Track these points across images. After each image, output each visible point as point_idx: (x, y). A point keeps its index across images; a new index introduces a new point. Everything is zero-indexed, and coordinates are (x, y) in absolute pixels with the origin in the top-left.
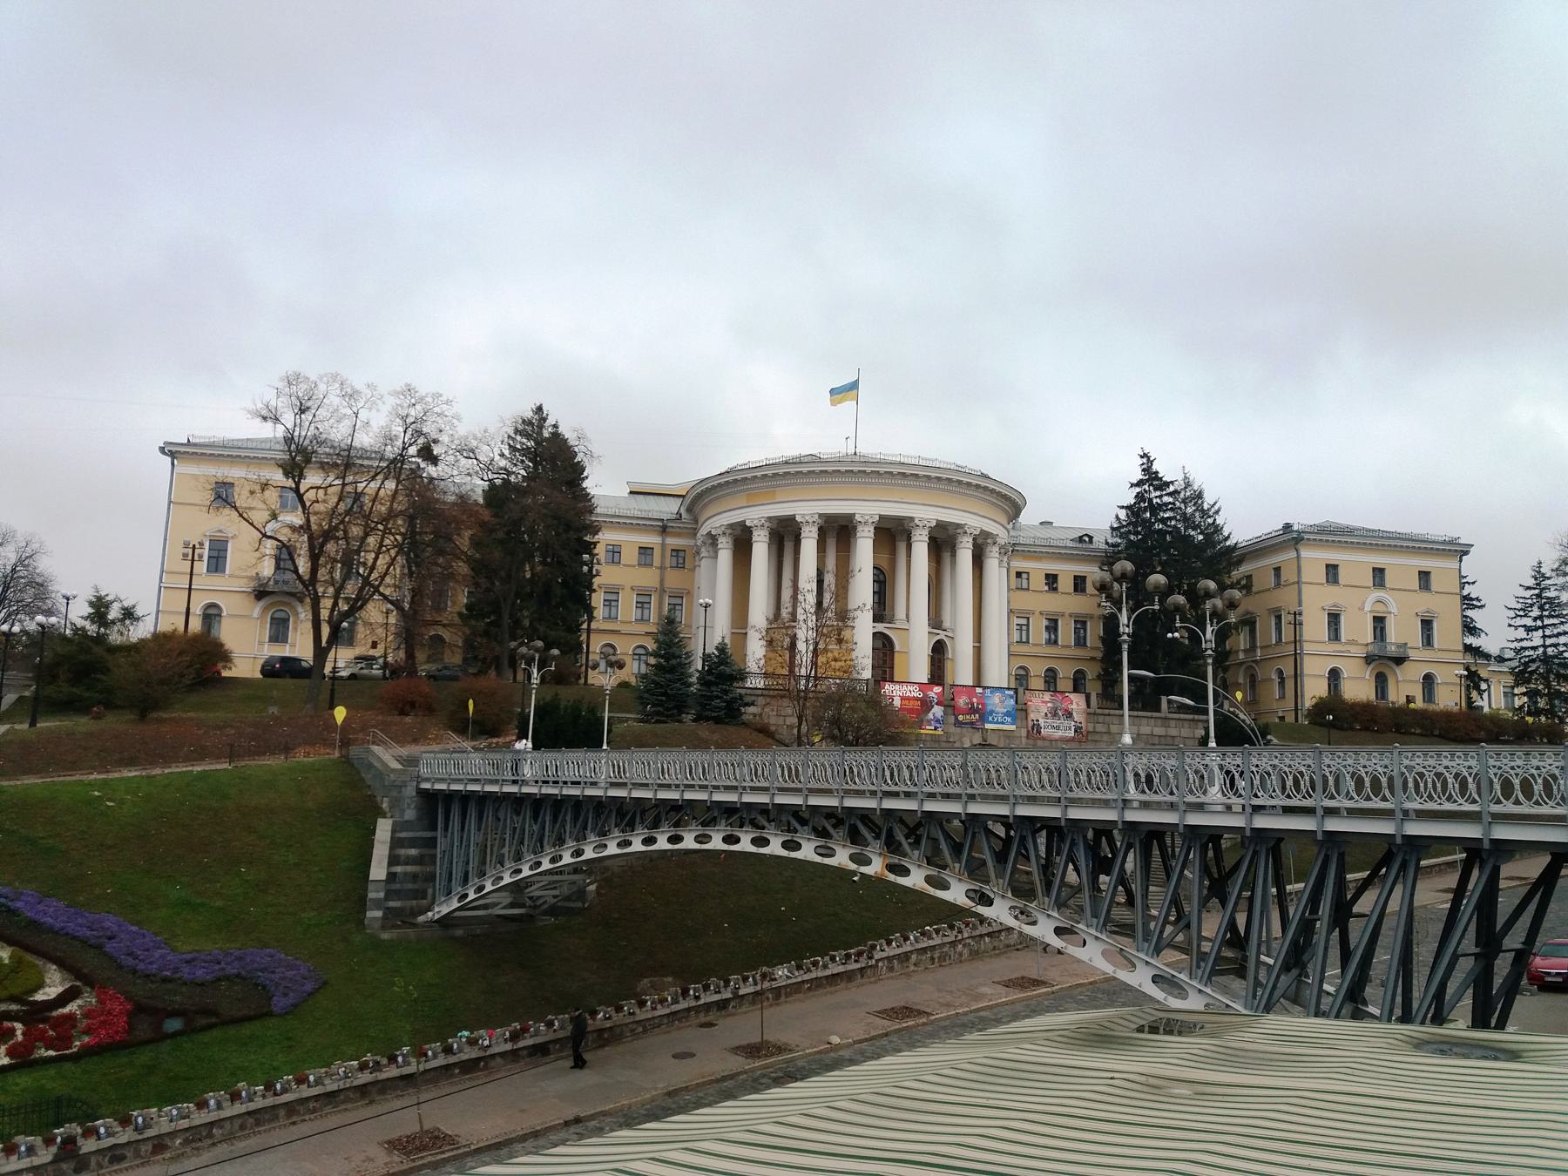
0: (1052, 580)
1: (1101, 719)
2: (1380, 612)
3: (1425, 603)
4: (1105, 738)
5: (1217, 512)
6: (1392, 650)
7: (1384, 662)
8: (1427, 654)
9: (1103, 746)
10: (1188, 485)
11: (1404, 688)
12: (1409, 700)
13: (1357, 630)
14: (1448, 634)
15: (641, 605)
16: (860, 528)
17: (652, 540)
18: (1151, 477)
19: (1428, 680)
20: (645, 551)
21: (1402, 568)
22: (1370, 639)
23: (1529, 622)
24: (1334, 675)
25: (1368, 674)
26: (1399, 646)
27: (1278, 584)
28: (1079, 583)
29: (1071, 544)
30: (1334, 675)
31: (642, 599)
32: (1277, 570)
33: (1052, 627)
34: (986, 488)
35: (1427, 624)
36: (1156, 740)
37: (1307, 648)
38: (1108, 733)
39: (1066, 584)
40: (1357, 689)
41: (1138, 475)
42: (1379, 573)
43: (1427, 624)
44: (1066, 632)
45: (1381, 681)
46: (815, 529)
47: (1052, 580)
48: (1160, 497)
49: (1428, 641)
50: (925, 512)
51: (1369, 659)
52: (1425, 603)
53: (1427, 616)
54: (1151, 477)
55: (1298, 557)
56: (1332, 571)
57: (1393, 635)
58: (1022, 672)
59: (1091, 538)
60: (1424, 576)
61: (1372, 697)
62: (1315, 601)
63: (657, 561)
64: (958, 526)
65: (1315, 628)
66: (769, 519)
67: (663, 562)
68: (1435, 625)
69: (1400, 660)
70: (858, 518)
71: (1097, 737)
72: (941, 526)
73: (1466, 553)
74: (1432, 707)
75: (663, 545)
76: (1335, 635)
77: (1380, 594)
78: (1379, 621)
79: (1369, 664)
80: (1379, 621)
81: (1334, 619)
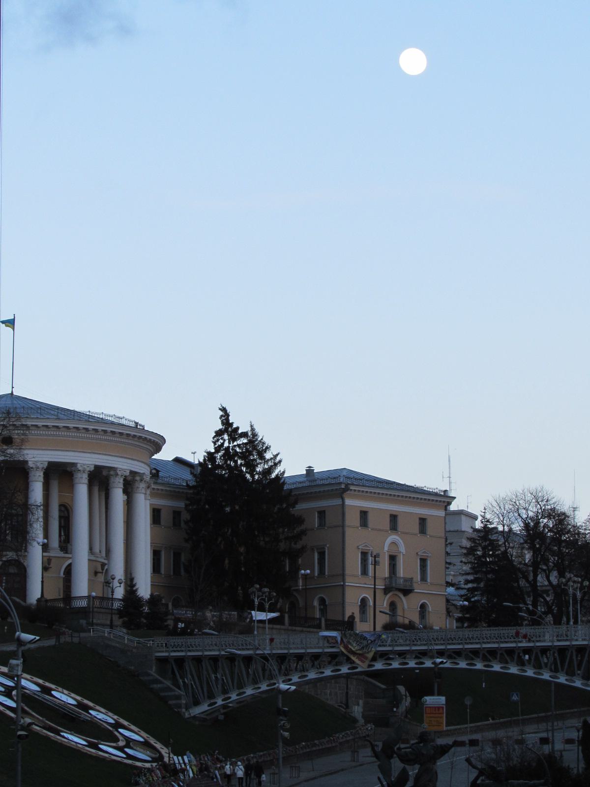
10: (254, 435)
16: (78, 476)
19: (423, 607)
26: (406, 580)
27: (322, 524)
32: (322, 514)
34: (140, 437)
35: (423, 561)
43: (423, 561)
46: (42, 474)
49: (424, 578)
54: (228, 428)
56: (364, 514)
57: (401, 572)
59: (158, 471)
62: (355, 540)
65: (353, 563)
68: (429, 563)
69: (407, 592)
72: (98, 469)
77: (393, 537)
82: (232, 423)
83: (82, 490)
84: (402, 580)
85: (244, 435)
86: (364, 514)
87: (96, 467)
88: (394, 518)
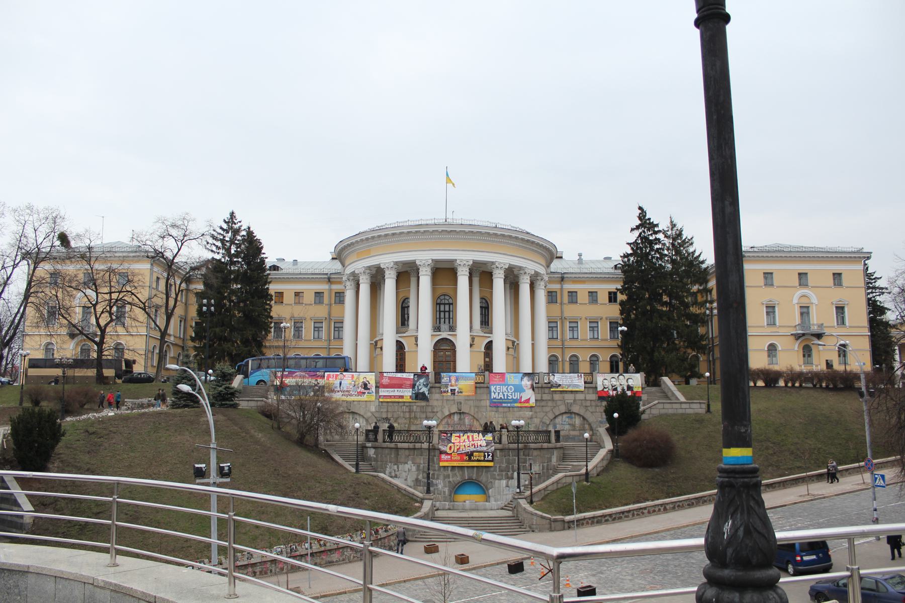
0: (593, 295)
1: (547, 391)
2: (804, 302)
3: (838, 295)
4: (550, 404)
5: (692, 244)
6: (815, 329)
7: (808, 339)
8: (842, 331)
9: (548, 409)
10: (673, 226)
12: (829, 365)
13: (789, 318)
14: (858, 316)
15: (317, 329)
17: (323, 287)
18: (645, 223)
20: (319, 295)
21: (820, 272)
22: (798, 321)
24: (772, 348)
25: (797, 346)
28: (612, 297)
29: (613, 271)
31: (317, 325)
35: (840, 309)
36: (588, 404)
38: (553, 400)
39: (603, 298)
42: (802, 276)
43: (840, 309)
44: (604, 330)
45: (807, 351)
47: (593, 295)
49: (841, 321)
50: (464, 257)
51: (797, 337)
52: (838, 295)
53: (840, 304)
54: (645, 223)
56: (768, 276)
57: (815, 319)
58: (574, 359)
60: (837, 276)
63: (326, 300)
64: (493, 263)
66: (369, 268)
67: (330, 301)
68: (846, 309)
69: (819, 336)
70: (418, 263)
71: (543, 403)
73: (868, 258)
75: (330, 290)
78: (805, 311)
79: (797, 339)
80: (805, 311)
81: (771, 310)
82: (649, 219)
83: (425, 281)
84: (816, 327)
85: (657, 225)
86: (768, 276)
87: (436, 261)
88: (802, 276)
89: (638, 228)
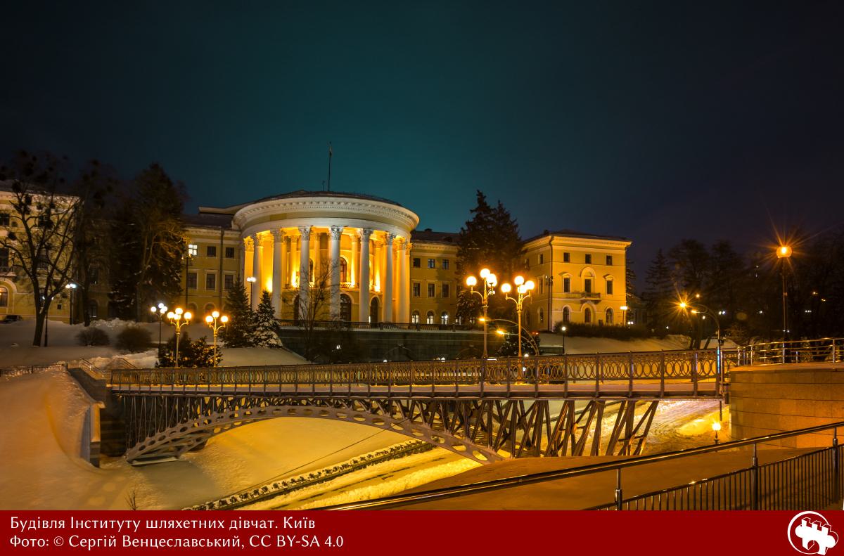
11: (599, 315)
23: (655, 280)
27: (542, 262)
30: (566, 311)
33: (432, 288)
35: (609, 284)
37: (554, 295)
40: (577, 316)
41: (475, 205)
48: (486, 217)
55: (552, 249)
61: (584, 320)
74: (610, 324)
75: (222, 244)
76: (567, 289)
78: (588, 283)
81: (567, 282)
89: (476, 210)
